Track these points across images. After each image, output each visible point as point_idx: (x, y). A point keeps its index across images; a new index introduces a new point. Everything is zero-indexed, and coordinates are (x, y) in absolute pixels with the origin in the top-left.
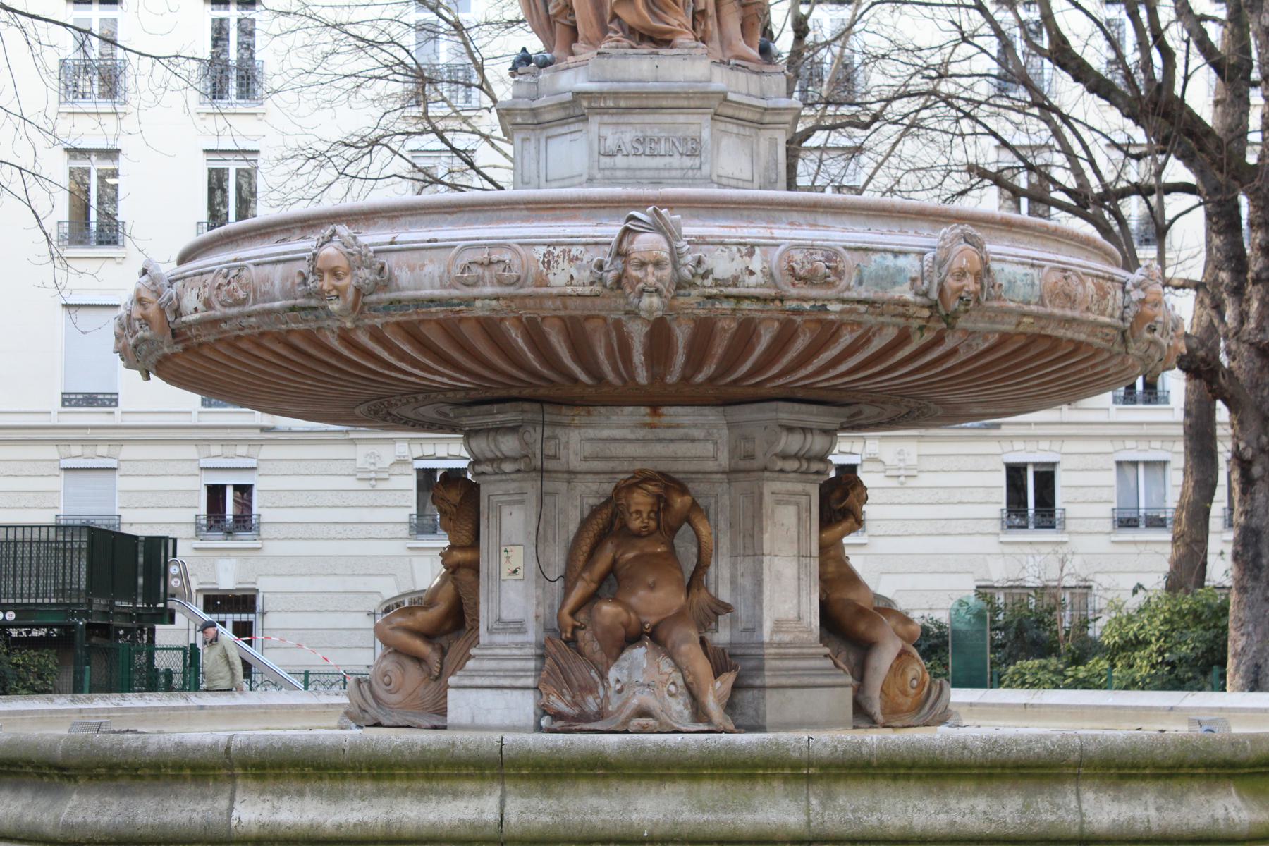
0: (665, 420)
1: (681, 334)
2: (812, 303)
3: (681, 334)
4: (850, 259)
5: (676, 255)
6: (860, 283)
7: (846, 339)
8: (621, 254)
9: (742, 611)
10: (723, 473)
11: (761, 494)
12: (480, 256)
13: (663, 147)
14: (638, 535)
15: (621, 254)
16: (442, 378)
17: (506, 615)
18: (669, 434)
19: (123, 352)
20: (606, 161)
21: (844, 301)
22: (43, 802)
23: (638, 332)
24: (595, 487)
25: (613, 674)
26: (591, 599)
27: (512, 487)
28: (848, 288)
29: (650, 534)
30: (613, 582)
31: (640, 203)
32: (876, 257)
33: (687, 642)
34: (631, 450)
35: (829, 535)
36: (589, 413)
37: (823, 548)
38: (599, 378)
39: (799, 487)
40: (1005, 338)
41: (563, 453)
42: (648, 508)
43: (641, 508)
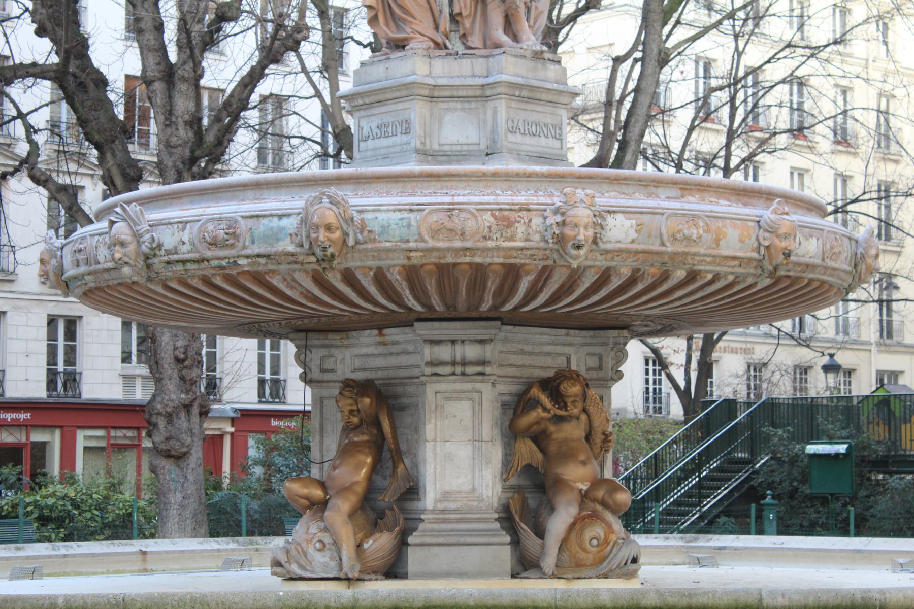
2: (227, 261)
4: (243, 225)
6: (253, 243)
21: (247, 257)
28: (244, 247)
32: (265, 221)
38: (429, 307)
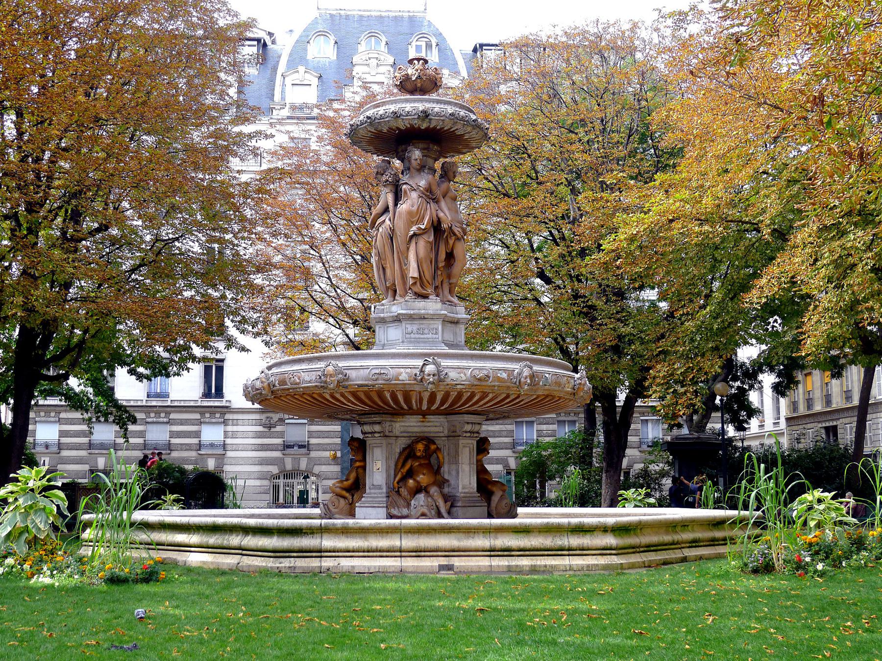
1: (439, 397)
3: (439, 397)
5: (439, 372)
7: (491, 396)
8: (422, 371)
9: (452, 482)
12: (377, 371)
13: (426, 331)
14: (419, 457)
15: (422, 371)
16: (360, 407)
17: (375, 483)
18: (428, 424)
19: (246, 396)
20: (408, 336)
22: (280, 540)
23: (426, 396)
25: (413, 502)
26: (404, 479)
27: (378, 441)
30: (410, 474)
31: (429, 355)
33: (434, 490)
35: (480, 457)
37: (477, 461)
39: (470, 441)
40: (538, 396)
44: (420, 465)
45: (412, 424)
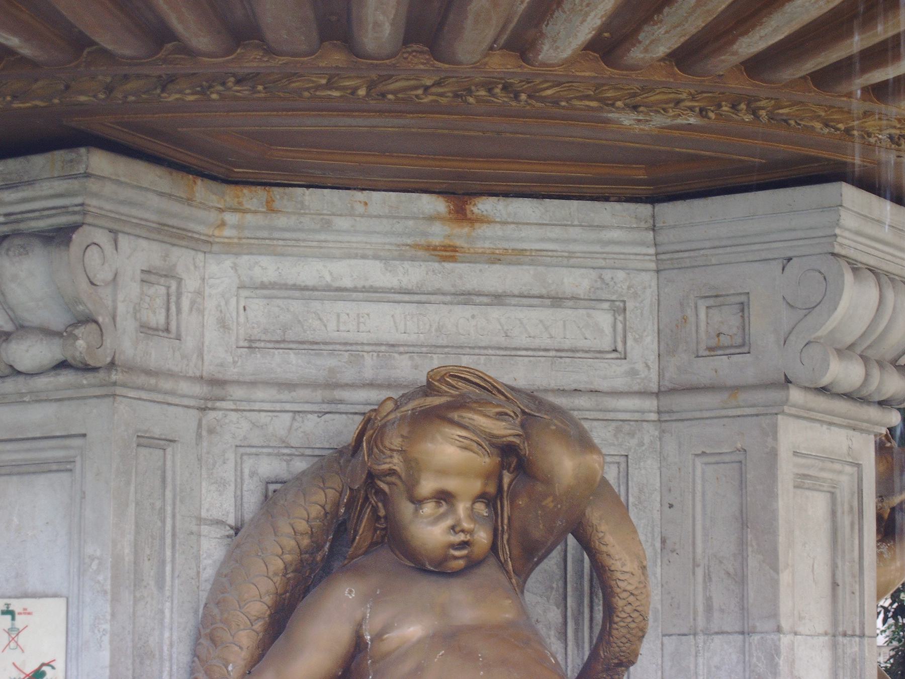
0: (487, 237)
10: (642, 394)
11: (773, 455)
18: (492, 278)
24: (280, 424)
27: (36, 416)
29: (473, 564)
34: (384, 322)
36: (271, 209)
39: (837, 440)
41: (189, 321)
42: (477, 486)
43: (451, 484)
44: (450, 639)
45: (345, 272)
